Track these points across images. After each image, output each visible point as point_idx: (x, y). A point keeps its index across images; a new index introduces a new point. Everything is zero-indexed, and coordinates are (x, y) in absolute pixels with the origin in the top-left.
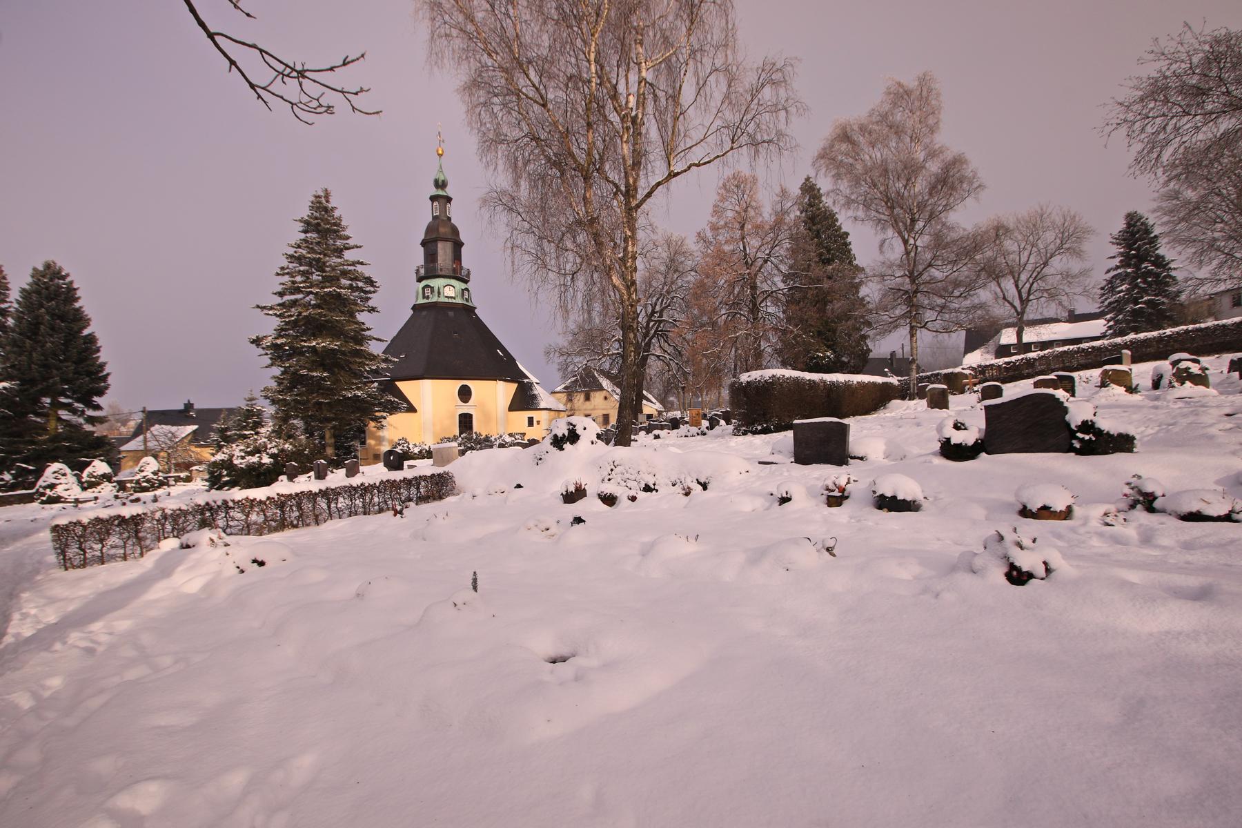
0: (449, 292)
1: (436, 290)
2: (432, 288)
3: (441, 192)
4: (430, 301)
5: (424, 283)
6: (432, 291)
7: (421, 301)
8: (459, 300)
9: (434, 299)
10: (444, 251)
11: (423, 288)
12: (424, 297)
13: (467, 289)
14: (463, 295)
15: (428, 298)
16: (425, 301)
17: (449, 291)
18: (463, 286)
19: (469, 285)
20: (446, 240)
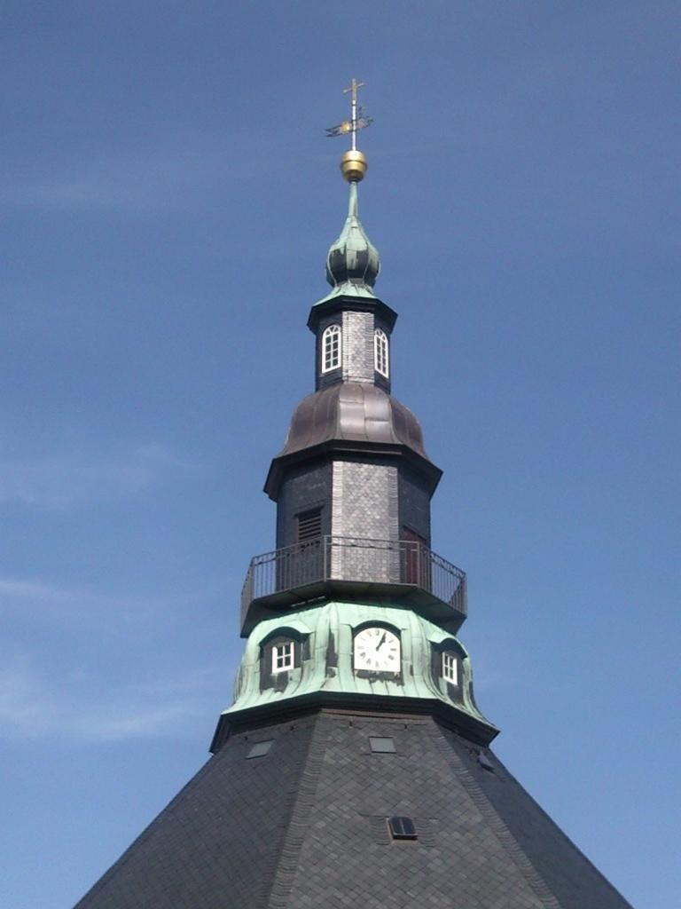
0: (375, 652)
1: (318, 645)
2: (302, 639)
3: (350, 290)
4: (290, 692)
5: (264, 629)
6: (303, 657)
7: (252, 698)
8: (418, 689)
9: (311, 683)
10: (359, 500)
11: (265, 645)
12: (266, 682)
13: (451, 648)
14: (436, 672)
15: (283, 681)
16: (271, 697)
17: (377, 651)
18: (439, 635)
19: (462, 638)
20: (362, 451)
